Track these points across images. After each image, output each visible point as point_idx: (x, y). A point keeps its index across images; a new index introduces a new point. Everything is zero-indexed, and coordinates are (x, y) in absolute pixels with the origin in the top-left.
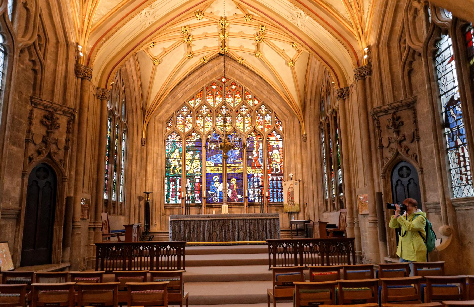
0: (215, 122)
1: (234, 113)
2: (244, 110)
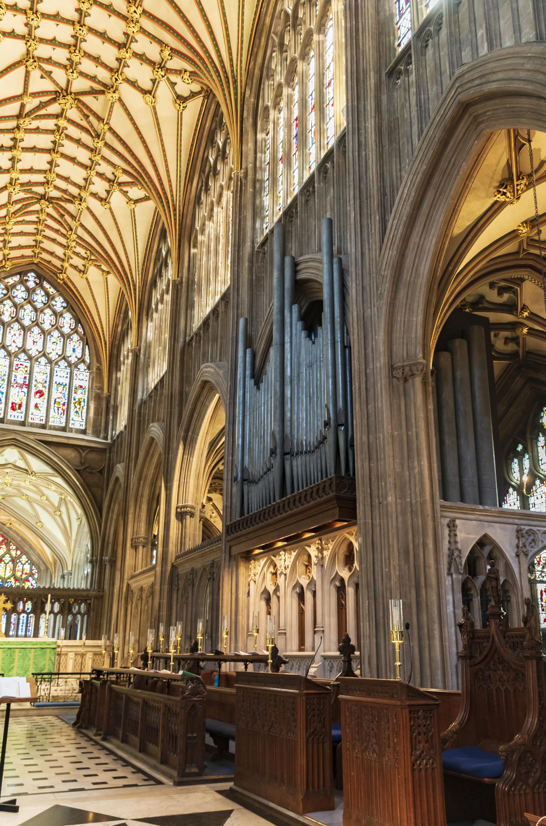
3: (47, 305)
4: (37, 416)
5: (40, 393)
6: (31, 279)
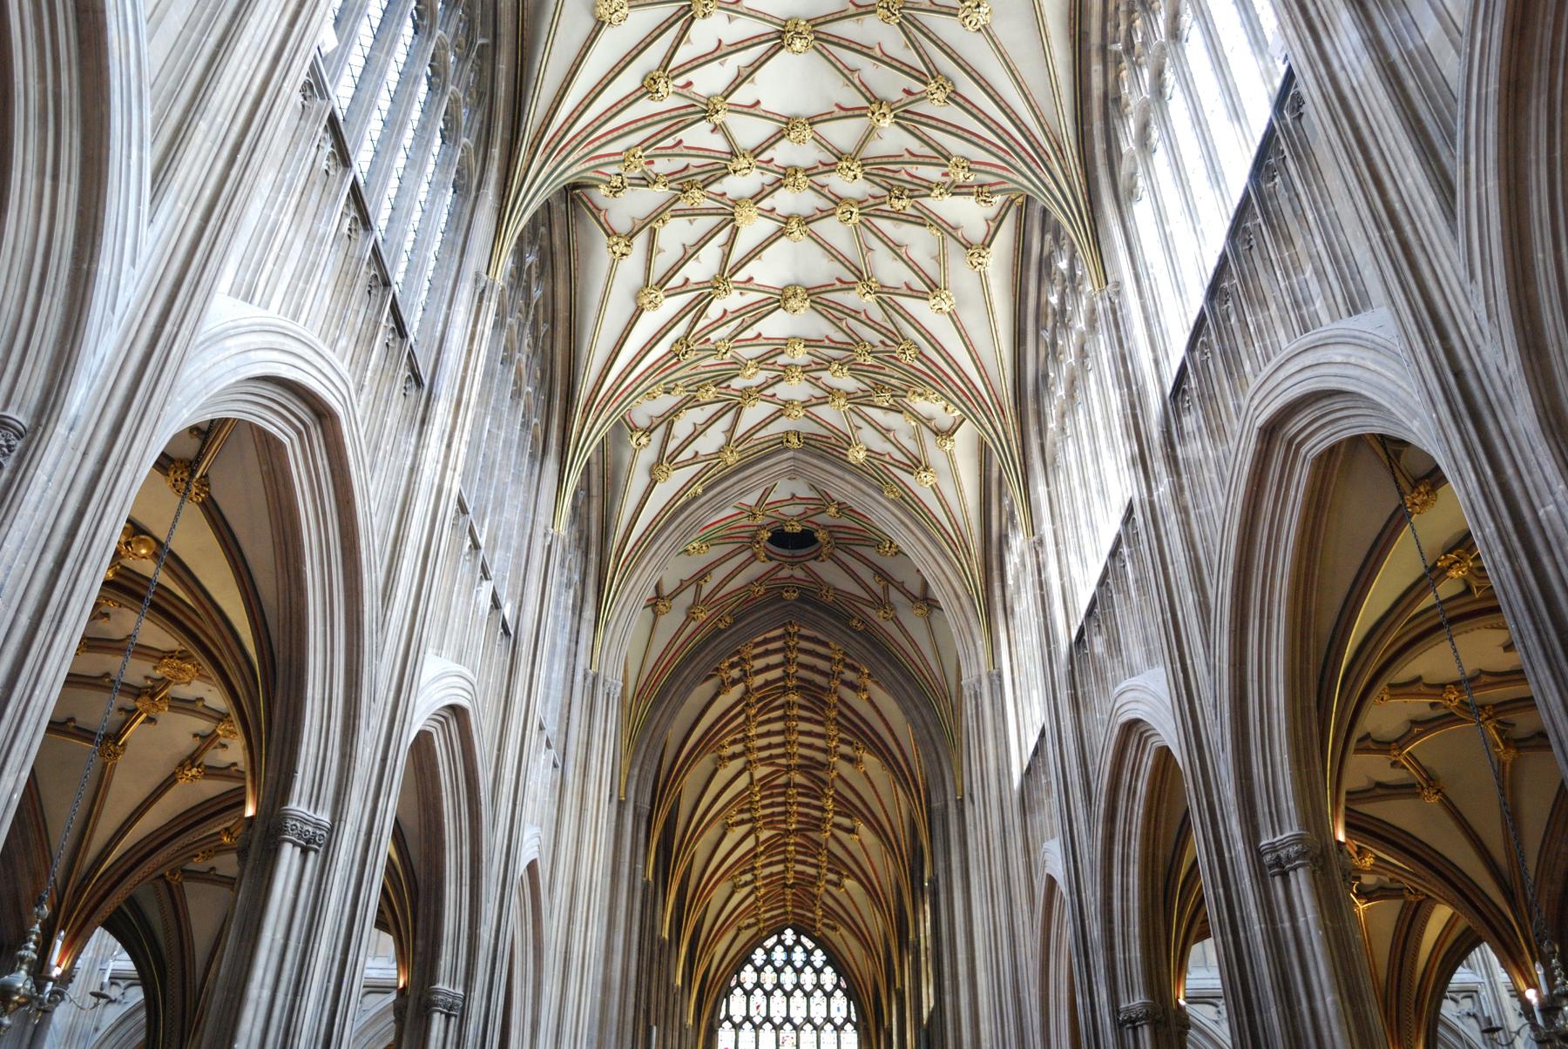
3: (808, 962)
6: (789, 936)
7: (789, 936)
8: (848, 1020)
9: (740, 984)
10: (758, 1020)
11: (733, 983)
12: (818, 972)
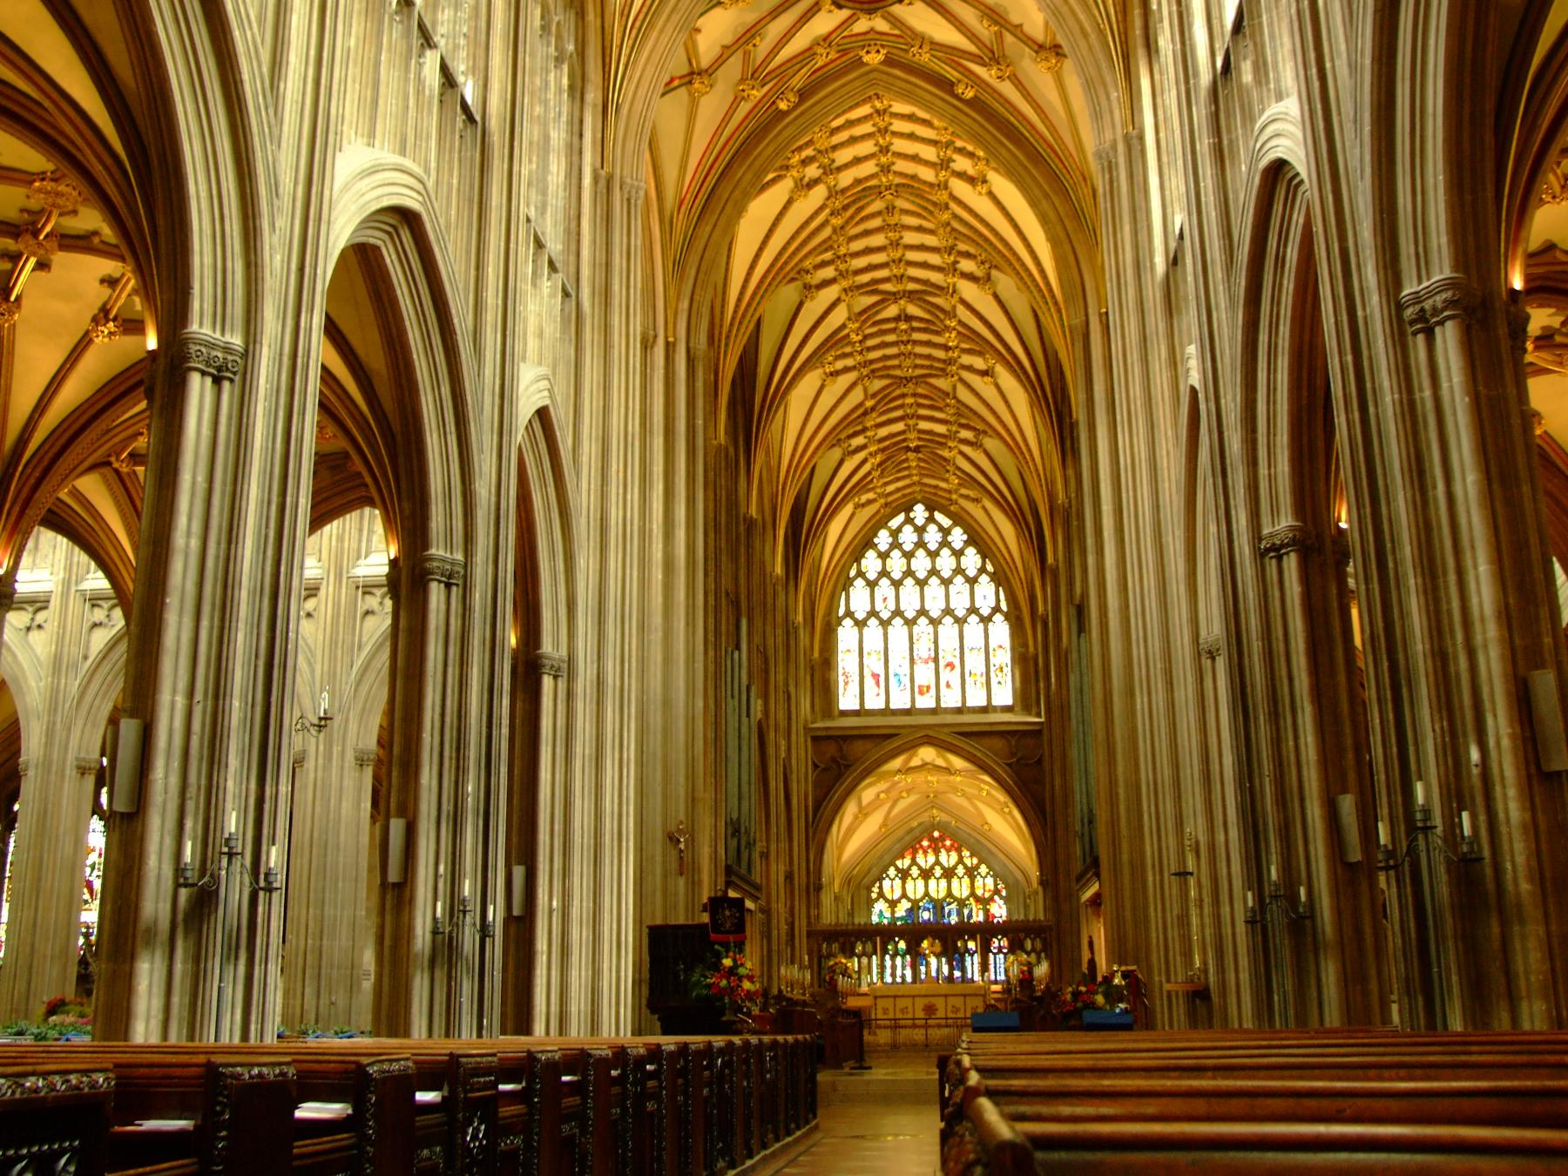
0: (926, 886)
1: (949, 874)
2: (960, 870)
3: (944, 543)
4: (951, 699)
5: (951, 665)
6: (919, 513)
7: (919, 513)
8: (996, 609)
9: (860, 574)
10: (885, 615)
11: (853, 573)
12: (958, 554)
